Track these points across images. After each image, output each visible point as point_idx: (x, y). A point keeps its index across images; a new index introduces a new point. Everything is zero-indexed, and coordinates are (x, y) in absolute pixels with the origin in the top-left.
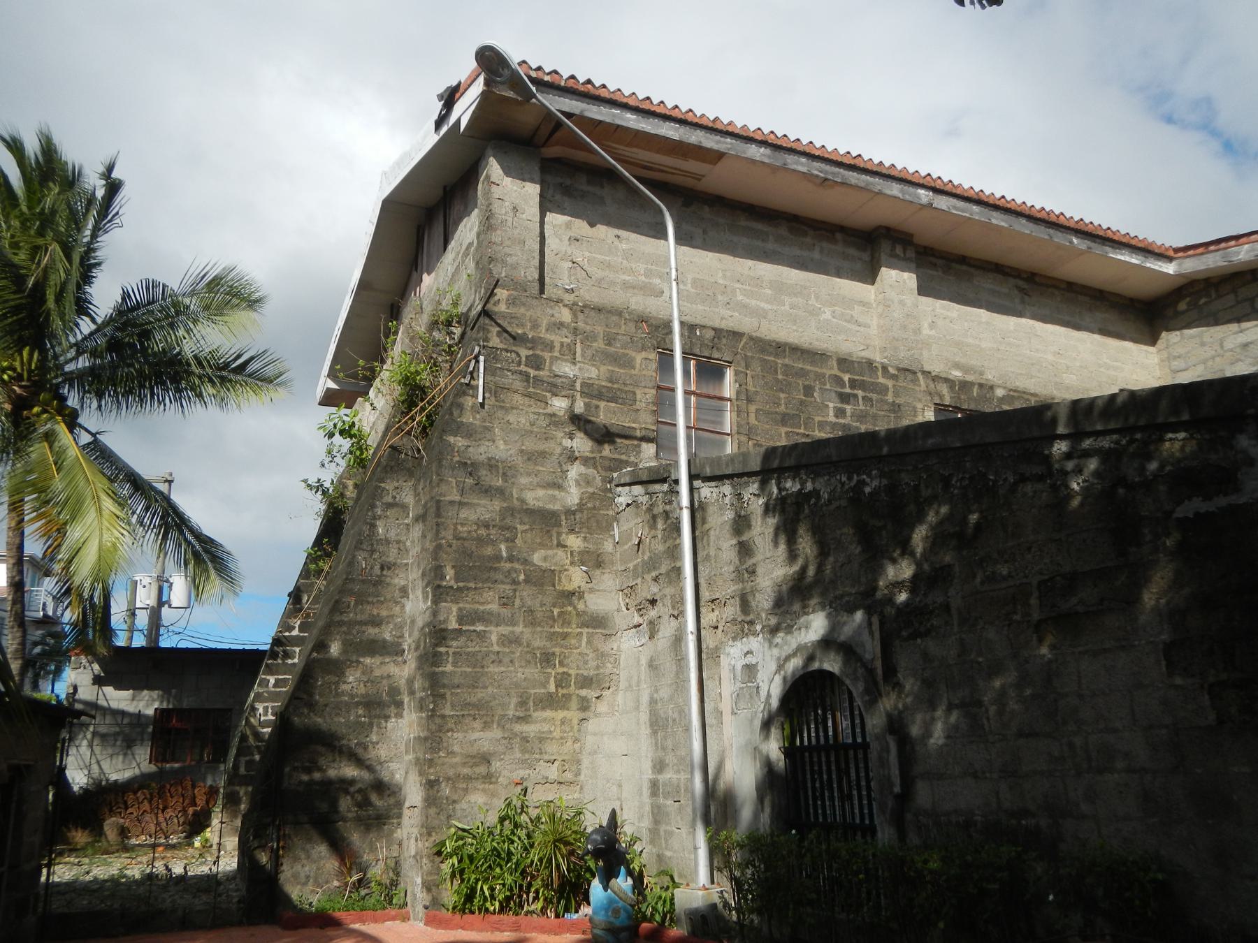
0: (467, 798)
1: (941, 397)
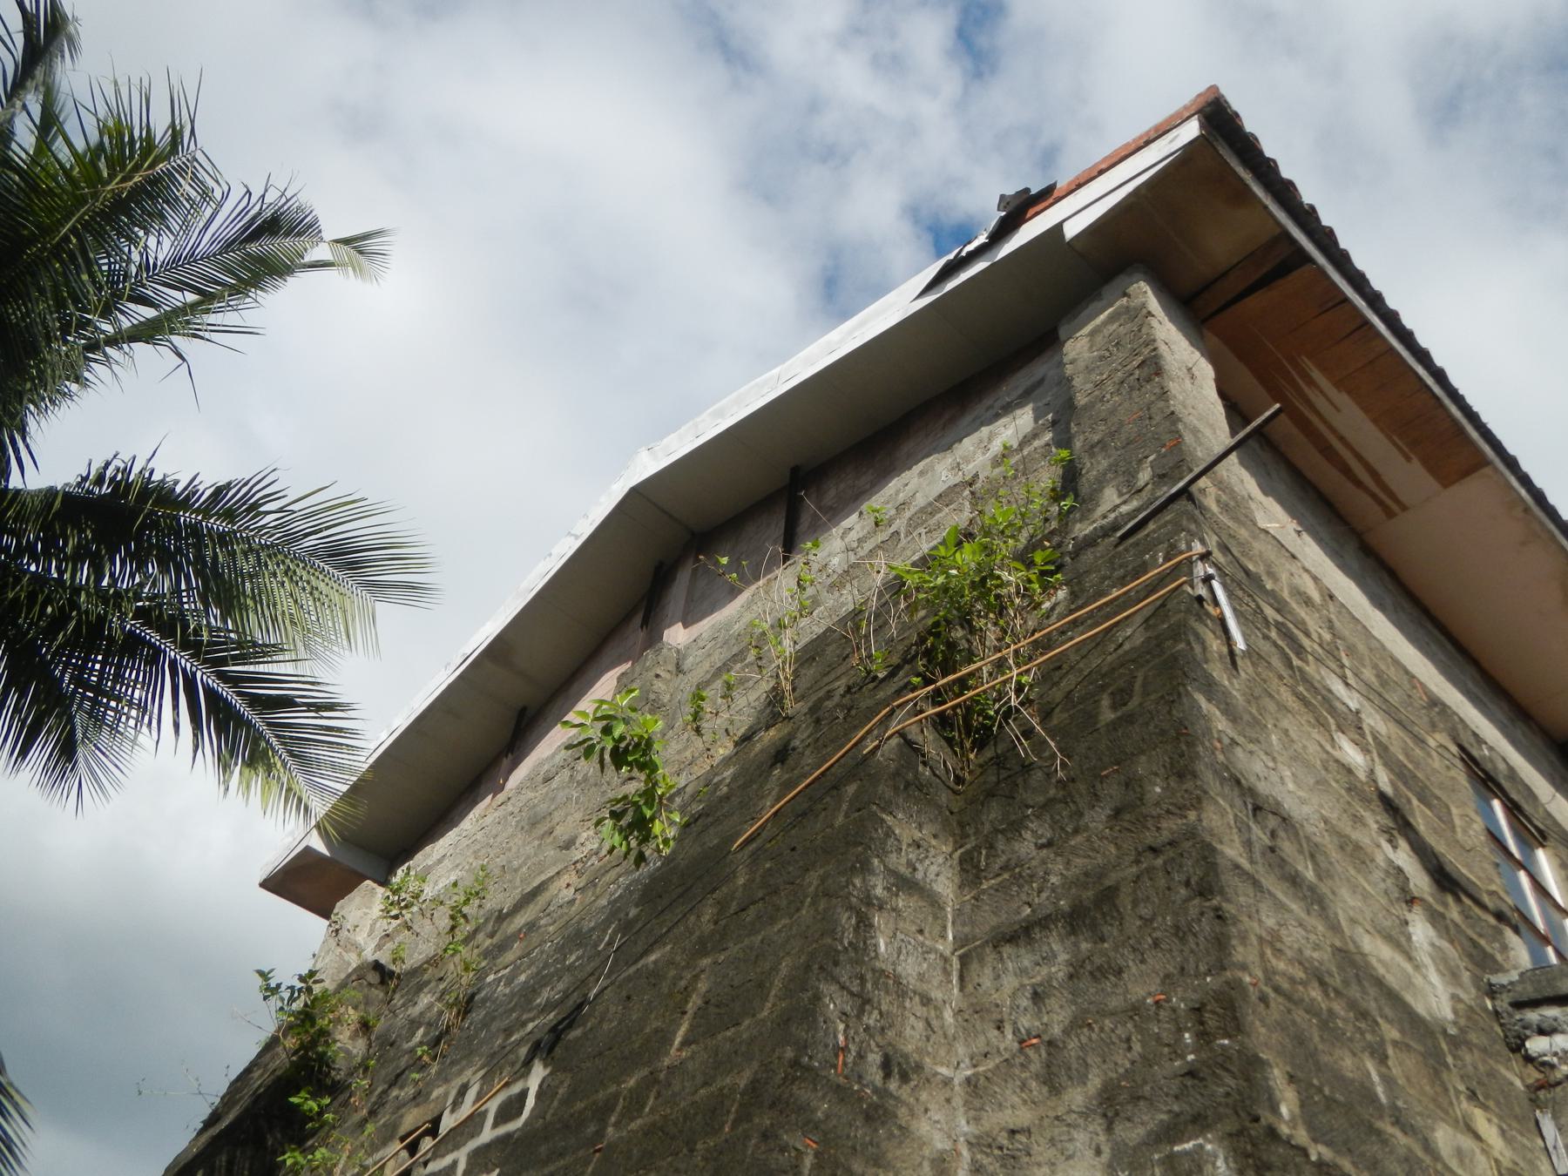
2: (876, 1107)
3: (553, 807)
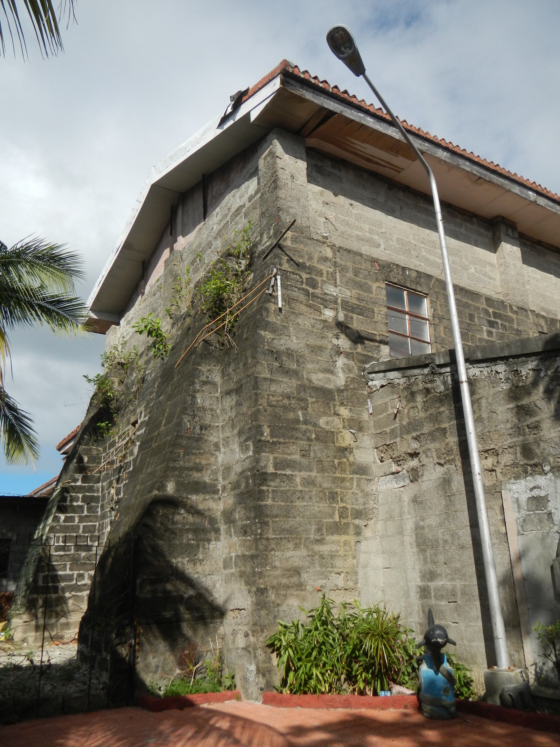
0: (287, 602)
1: (542, 327)
2: (198, 438)
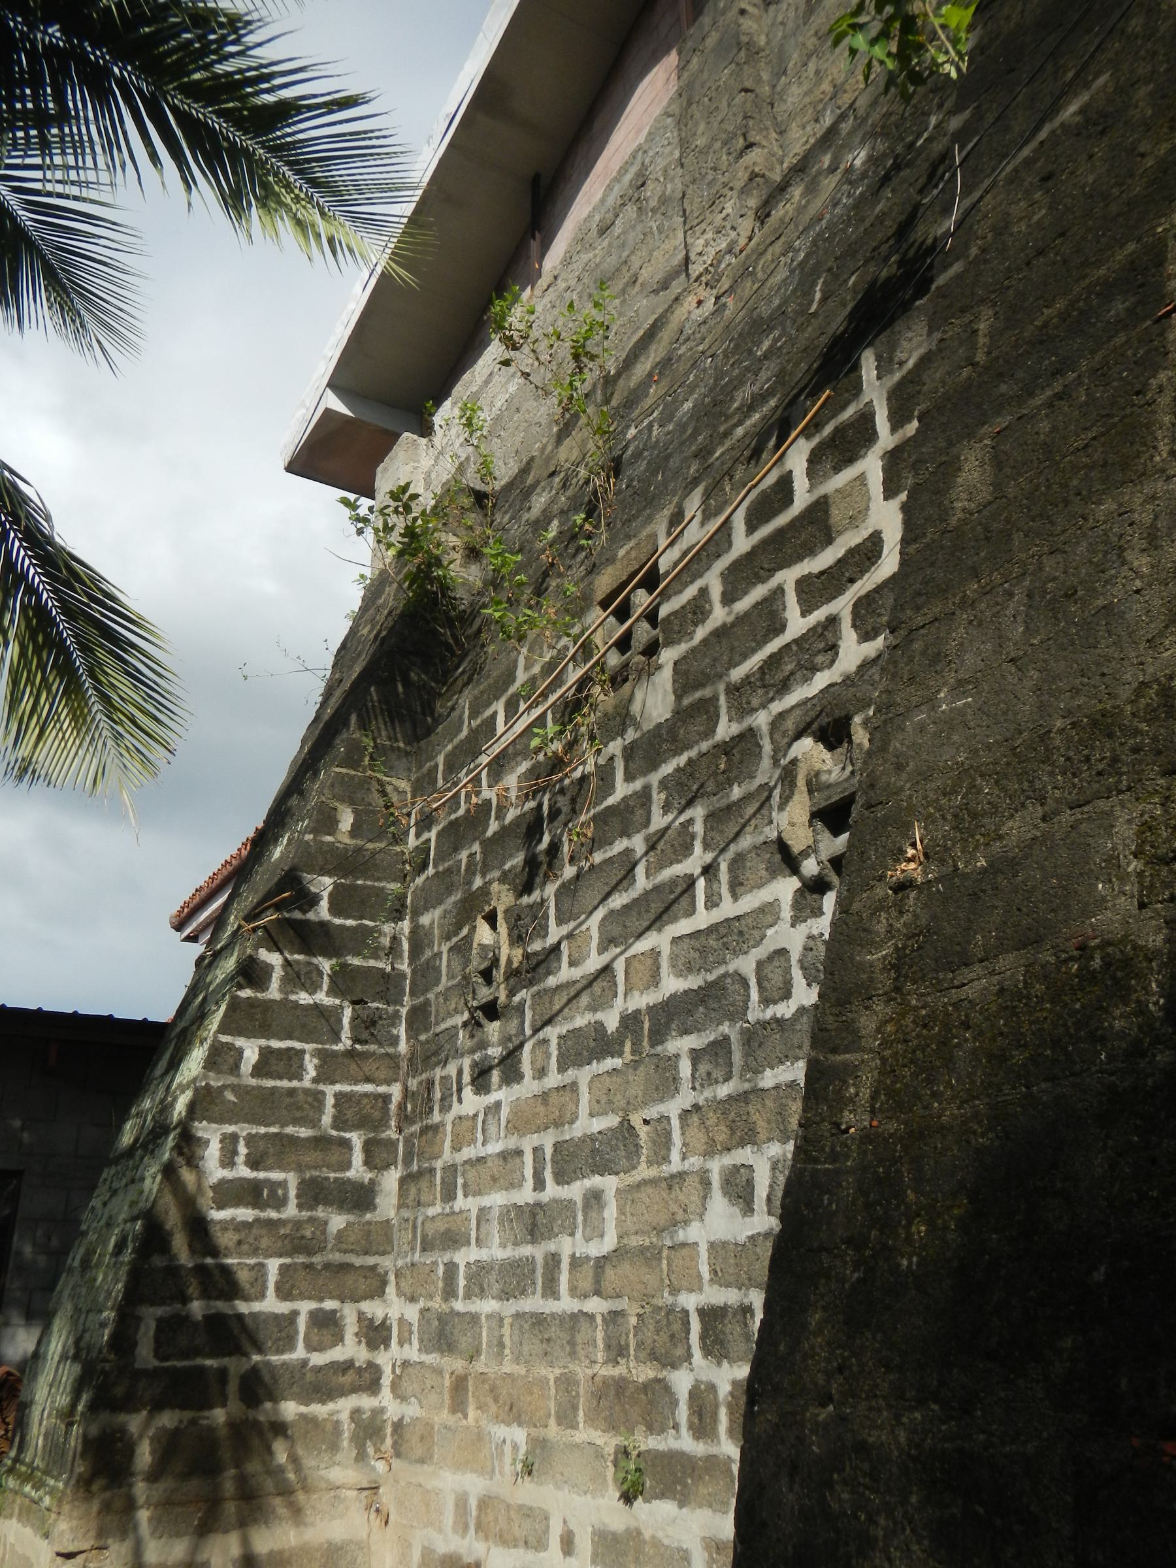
3: (626, 254)
